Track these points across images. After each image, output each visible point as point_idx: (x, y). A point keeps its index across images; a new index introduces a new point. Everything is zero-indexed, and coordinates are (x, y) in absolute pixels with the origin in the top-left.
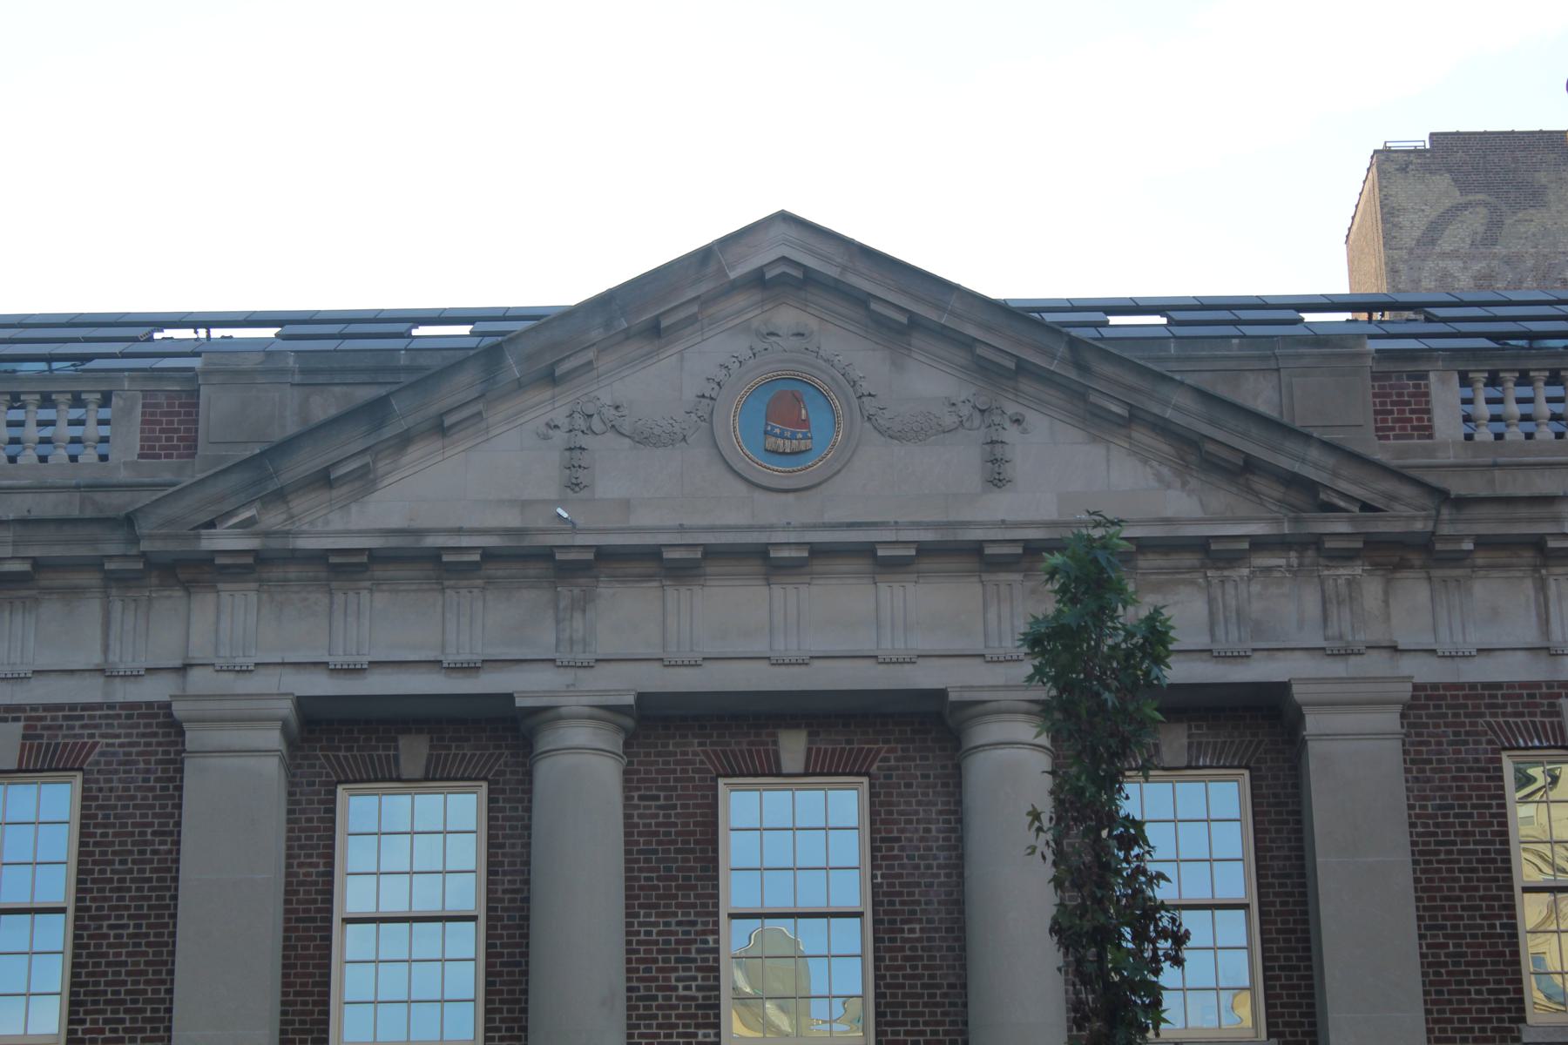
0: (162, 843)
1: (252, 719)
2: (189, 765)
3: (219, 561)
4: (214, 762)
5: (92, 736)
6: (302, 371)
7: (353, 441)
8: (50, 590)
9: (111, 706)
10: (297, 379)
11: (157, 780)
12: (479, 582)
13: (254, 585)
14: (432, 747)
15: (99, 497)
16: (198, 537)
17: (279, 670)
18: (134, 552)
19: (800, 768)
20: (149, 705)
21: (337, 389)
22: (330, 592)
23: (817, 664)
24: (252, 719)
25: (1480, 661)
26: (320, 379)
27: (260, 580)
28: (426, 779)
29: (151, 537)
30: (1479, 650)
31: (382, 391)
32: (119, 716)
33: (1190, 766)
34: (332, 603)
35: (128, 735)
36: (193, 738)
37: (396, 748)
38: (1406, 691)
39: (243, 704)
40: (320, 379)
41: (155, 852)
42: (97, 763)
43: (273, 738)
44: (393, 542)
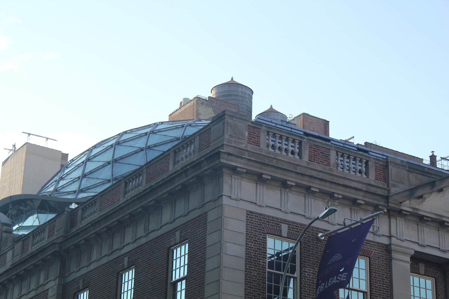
0: (387, 280)
1: (400, 252)
2: (393, 261)
3: (403, 212)
4: (397, 262)
5: (371, 249)
6: (409, 167)
7: (428, 189)
8: (362, 209)
9: (375, 242)
10: (407, 169)
11: (385, 264)
12: (446, 230)
13: (404, 219)
14: (425, 267)
15: (370, 187)
16: (401, 205)
17: (410, 243)
18: (386, 205)
19: (423, 274)
20: (382, 244)
21: (414, 174)
22: (439, 230)
23: (241, 202)
24: (400, 252)
25: (290, 215)
26: (412, 170)
27: (405, 219)
28: (424, 275)
29: (392, 203)
30: (266, 206)
31: (434, 180)
32: (376, 245)
33: (426, 274)
34: (418, 228)
35: (378, 251)
36: (394, 255)
37: (419, 266)
38: (413, 252)
39: (402, 249)
40: (412, 170)
41: (386, 282)
42: (373, 256)
43: (408, 259)
44: (437, 217)
